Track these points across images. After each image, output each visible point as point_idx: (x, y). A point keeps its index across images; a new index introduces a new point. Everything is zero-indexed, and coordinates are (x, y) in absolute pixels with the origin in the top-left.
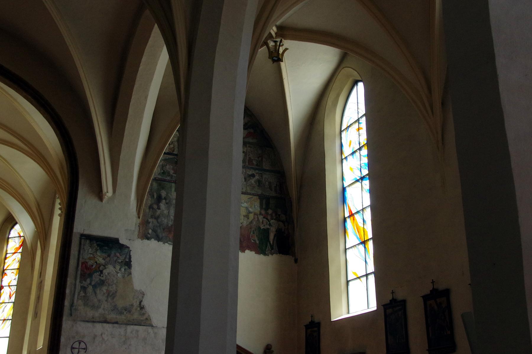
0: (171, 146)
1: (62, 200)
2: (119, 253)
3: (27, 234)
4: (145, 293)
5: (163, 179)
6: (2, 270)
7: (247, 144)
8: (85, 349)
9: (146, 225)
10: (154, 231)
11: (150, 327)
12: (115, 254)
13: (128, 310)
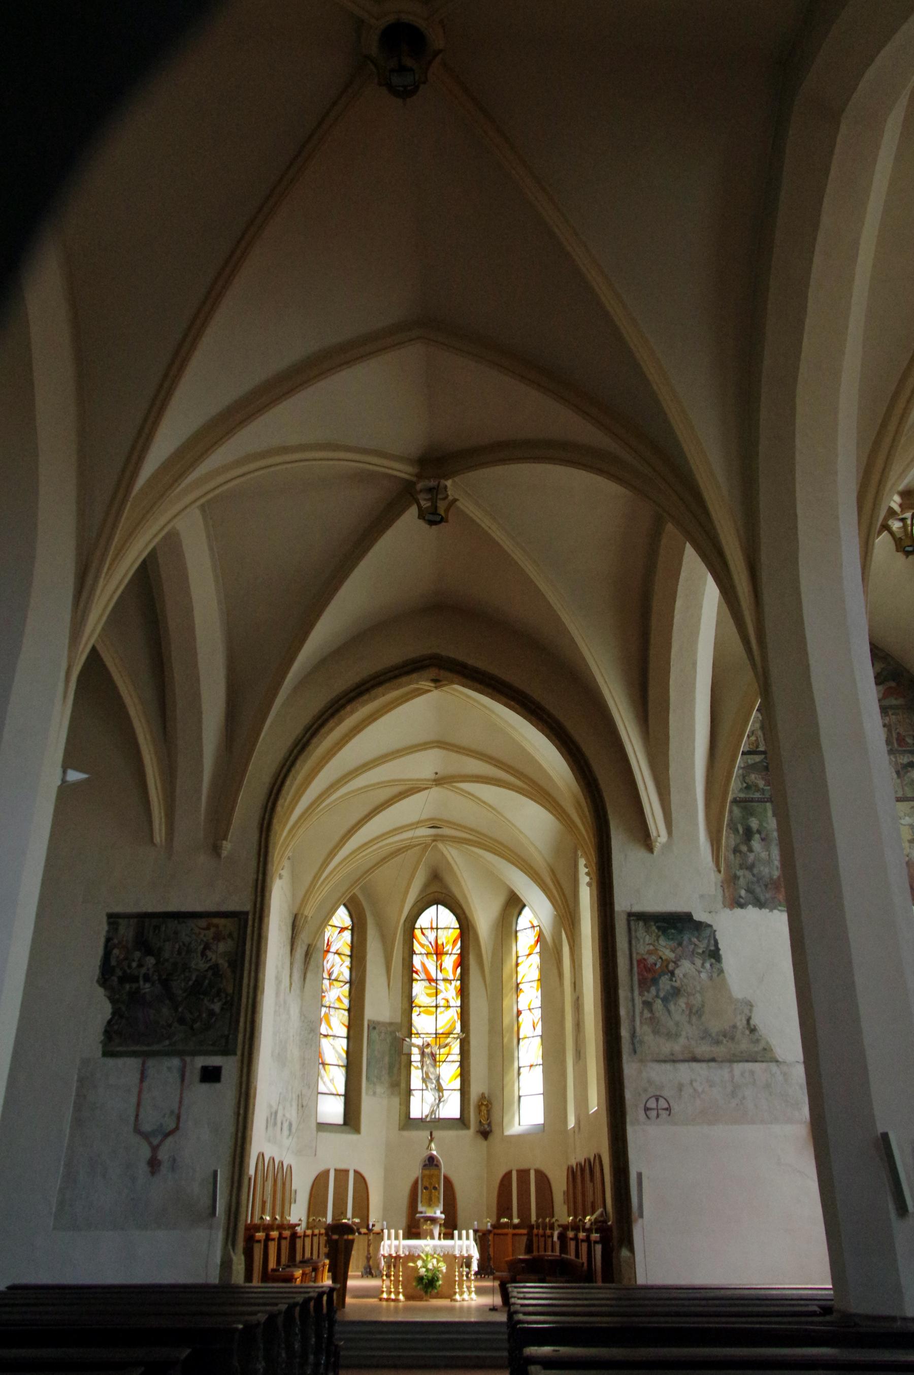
0: (751, 738)
1: (587, 859)
2: (698, 938)
3: (543, 921)
4: (754, 1004)
5: (749, 798)
6: (514, 985)
7: (888, 710)
8: (668, 1109)
9: (734, 884)
10: (748, 891)
11: (774, 1064)
12: (690, 940)
13: (729, 1035)
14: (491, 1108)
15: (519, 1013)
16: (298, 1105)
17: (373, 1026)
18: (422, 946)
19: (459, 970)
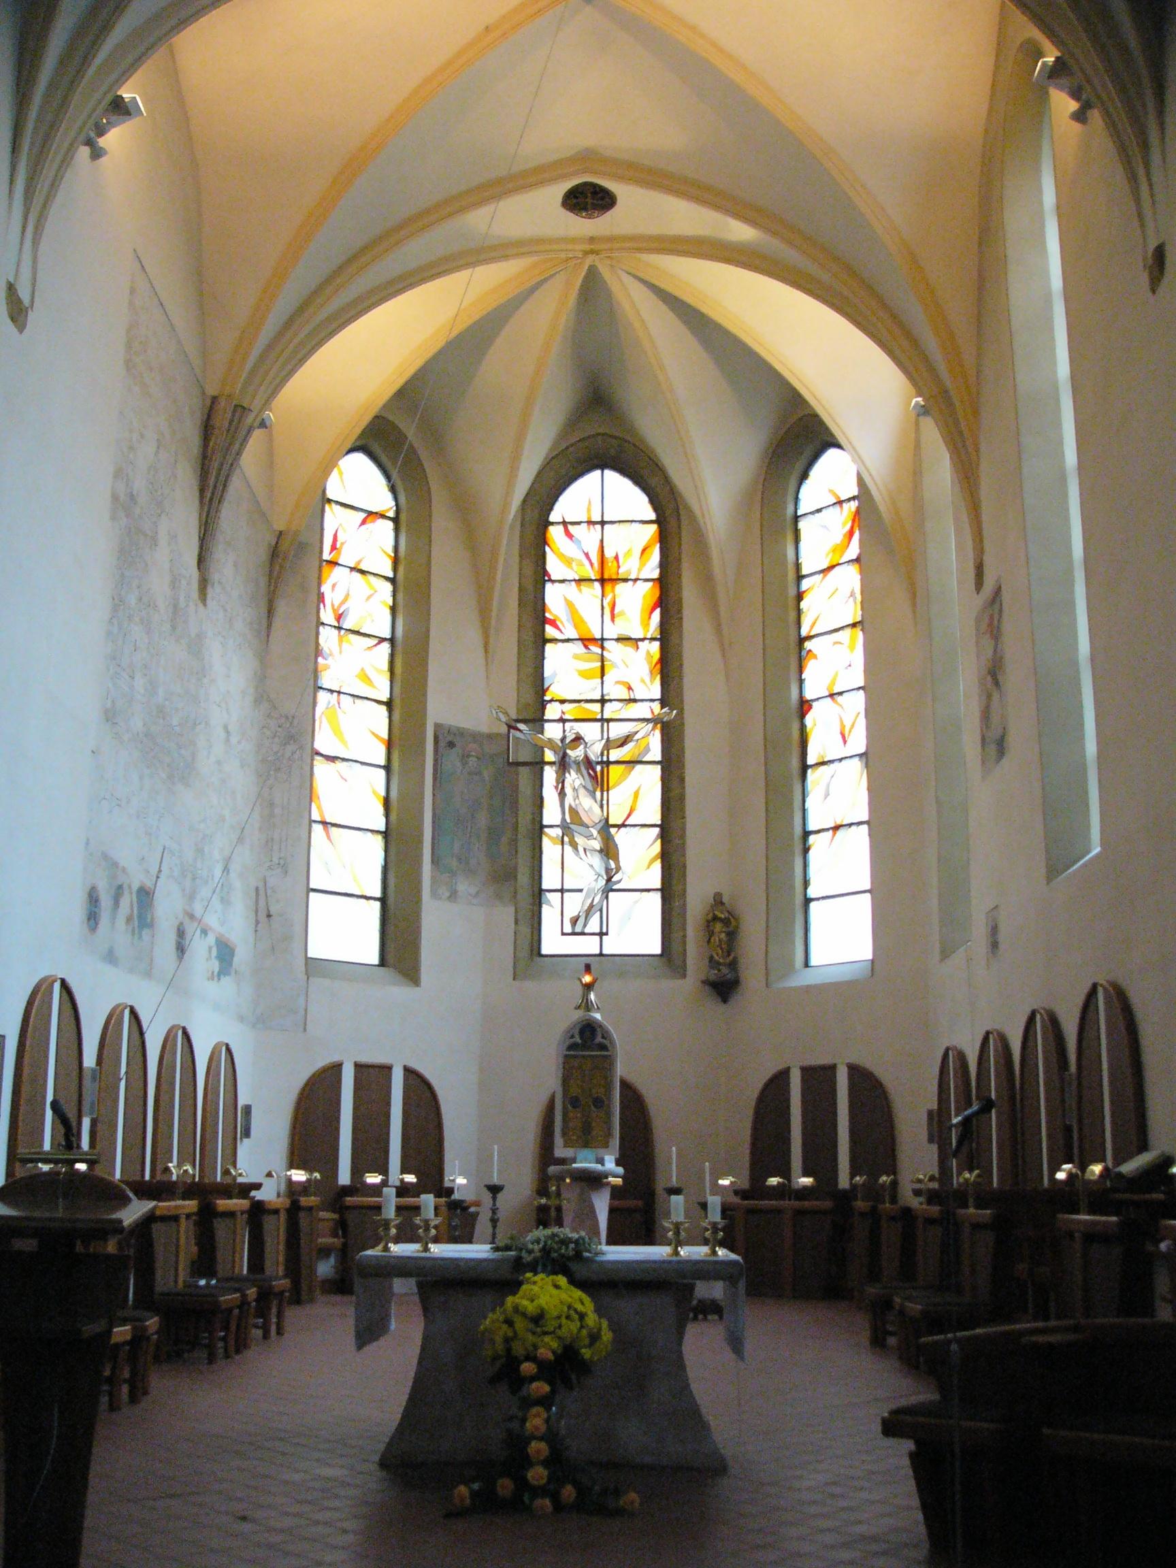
3: (868, 464)
6: (793, 639)
14: (737, 927)
15: (804, 706)
16: (257, 911)
17: (448, 739)
18: (568, 561)
19: (657, 614)
